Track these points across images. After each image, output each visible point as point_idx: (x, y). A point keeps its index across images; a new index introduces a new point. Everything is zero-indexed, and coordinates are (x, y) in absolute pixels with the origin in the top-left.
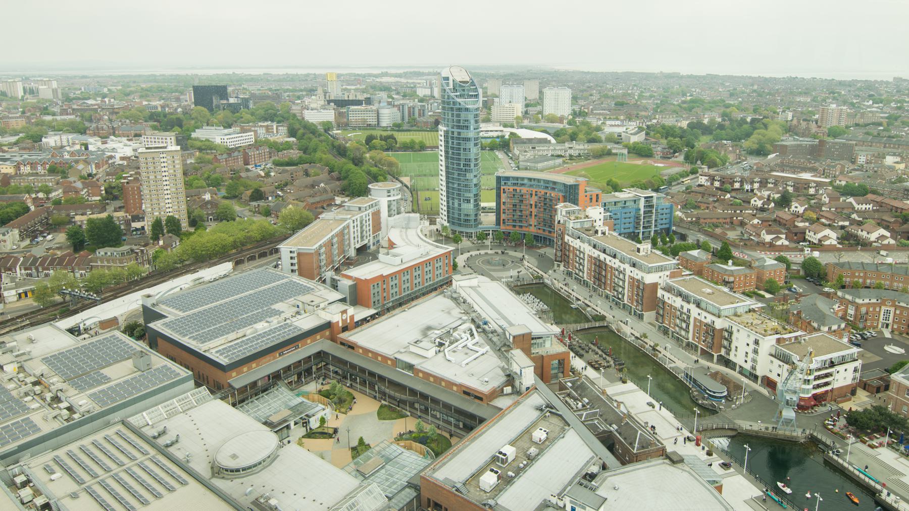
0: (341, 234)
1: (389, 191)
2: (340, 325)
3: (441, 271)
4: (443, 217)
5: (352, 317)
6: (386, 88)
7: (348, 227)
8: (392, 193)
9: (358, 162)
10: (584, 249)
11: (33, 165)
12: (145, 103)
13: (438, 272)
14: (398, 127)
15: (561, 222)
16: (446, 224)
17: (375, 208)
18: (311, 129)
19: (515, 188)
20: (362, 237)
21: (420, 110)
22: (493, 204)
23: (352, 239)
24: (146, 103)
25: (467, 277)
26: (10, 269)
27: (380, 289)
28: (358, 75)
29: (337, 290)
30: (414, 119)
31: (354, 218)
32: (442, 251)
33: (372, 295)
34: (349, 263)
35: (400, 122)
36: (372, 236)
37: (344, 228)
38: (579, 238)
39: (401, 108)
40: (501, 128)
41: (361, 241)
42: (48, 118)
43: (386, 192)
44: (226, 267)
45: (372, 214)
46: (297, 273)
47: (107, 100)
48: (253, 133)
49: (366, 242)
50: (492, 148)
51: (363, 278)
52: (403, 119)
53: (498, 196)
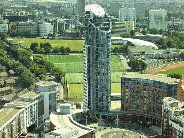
0: (19, 119)
10: (182, 130)
14: (51, 36)
15: (166, 111)
17: (41, 99)
21: (66, 25)
22: (119, 94)
30: (62, 31)
32: (87, 132)
35: (52, 33)
36: (38, 118)
38: (179, 123)
40: (120, 38)
50: (115, 51)
52: (54, 31)
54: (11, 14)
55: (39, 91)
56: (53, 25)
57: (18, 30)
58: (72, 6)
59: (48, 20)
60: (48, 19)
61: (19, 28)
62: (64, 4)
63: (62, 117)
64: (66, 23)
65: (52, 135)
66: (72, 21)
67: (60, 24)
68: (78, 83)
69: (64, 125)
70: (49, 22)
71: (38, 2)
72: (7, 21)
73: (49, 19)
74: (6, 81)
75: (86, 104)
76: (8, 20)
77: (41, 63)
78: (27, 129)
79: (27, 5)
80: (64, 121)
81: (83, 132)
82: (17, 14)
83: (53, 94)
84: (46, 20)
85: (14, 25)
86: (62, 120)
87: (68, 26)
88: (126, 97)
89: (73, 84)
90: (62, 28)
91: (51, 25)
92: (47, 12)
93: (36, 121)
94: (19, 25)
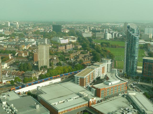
2: (91, 102)
3: (123, 88)
4: (124, 69)
5: (95, 100)
6: (108, 27)
7: (95, 71)
8: (109, 62)
9: (98, 51)
11: (11, 45)
12: (39, 29)
13: (122, 89)
16: (125, 73)
17: (103, 66)
18: (83, 38)
19: (149, 63)
20: (99, 74)
22: (142, 67)
23: (96, 75)
24: (40, 29)
26: (4, 74)
27: (104, 92)
29: (91, 91)
31: (97, 69)
33: (101, 94)
34: (95, 82)
36: (102, 74)
37: (94, 72)
39: (112, 34)
42: (15, 33)
43: (107, 61)
44: (59, 80)
46: (79, 84)
47: (30, 28)
48: (68, 39)
51: (99, 88)
52: (112, 37)
53: (143, 64)
67: (115, 34)
70: (110, 33)
72: (91, 32)
77: (105, 51)
82: (96, 29)
90: (116, 35)
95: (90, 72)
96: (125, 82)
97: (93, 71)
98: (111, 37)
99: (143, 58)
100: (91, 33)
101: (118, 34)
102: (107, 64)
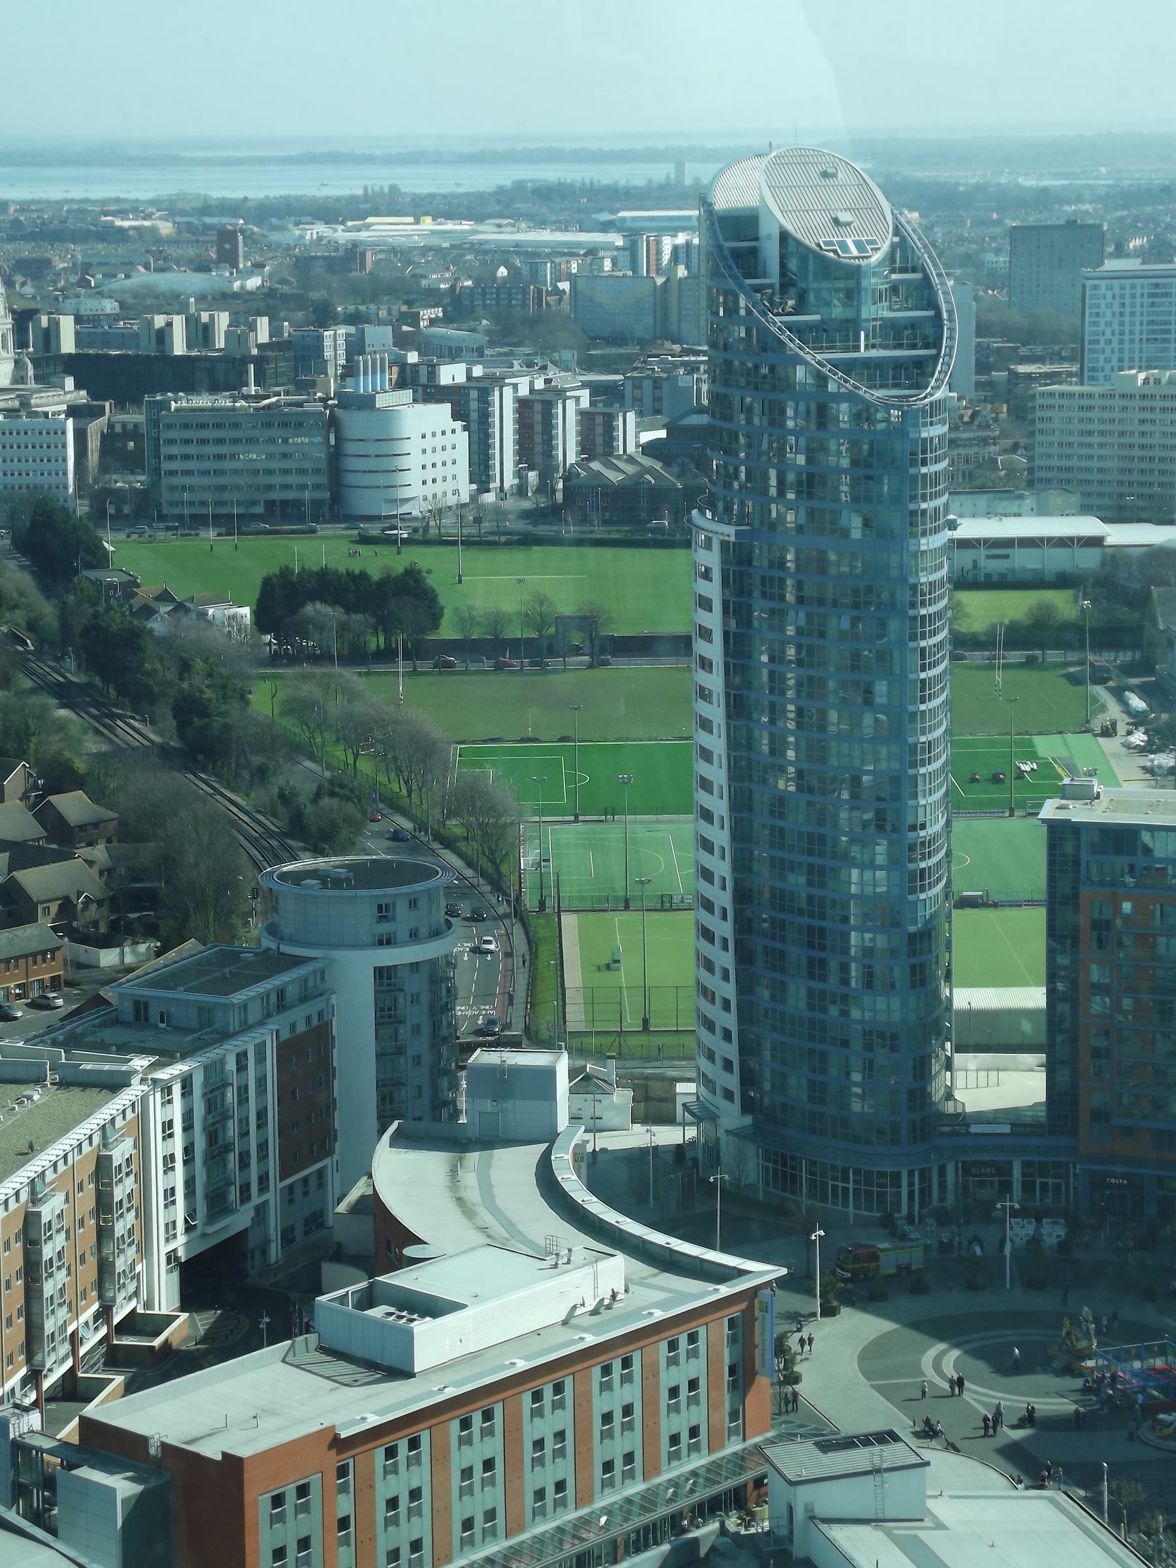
1: (384, 912)
17: (298, 1017)
22: (1035, 997)
25: (860, 1458)
28: (232, 208)
36: (276, 1184)
41: (211, 1218)
45: (283, 1049)
49: (240, 1220)
51: (211, 1450)
54: (107, 340)
55: (292, 941)
56: (474, 416)
57: (157, 471)
58: (658, 265)
59: (423, 379)
60: (423, 371)
61: (165, 450)
62: (592, 252)
63: (486, 1167)
64: (585, 403)
65: (377, 1312)
66: (648, 385)
68: (666, 904)
69: (499, 1231)
70: (430, 392)
71: (355, 244)
72: (70, 391)
73: (433, 373)
74: (20, 875)
75: (713, 1071)
76: (78, 386)
78: (176, 1275)
79: (260, 266)
80: (500, 1202)
81: (661, 1296)
82: (163, 336)
83: (415, 967)
84: (406, 379)
85: (124, 425)
86: (486, 1187)
87: (609, 429)
88: (1098, 1005)
89: (617, 918)
91: (455, 416)
92: (433, 322)
93: (261, 1210)
94: (170, 426)
95: (30, 1151)
96: (724, 1290)
97: (91, 1125)
98: (463, 469)
99: (1049, 810)
100: (73, 411)
101: (585, 417)
102: (383, 974)
